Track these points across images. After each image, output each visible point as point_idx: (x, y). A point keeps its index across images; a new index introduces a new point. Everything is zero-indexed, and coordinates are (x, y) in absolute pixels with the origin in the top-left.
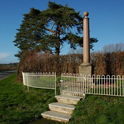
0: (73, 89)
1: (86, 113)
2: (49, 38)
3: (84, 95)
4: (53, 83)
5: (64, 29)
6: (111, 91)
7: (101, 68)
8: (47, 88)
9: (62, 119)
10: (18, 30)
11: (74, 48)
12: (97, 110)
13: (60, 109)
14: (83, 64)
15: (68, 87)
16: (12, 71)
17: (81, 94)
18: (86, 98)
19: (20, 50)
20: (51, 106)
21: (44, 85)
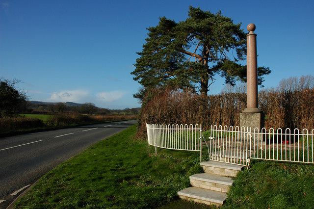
0: (230, 152)
1: (251, 191)
2: (191, 67)
3: (248, 161)
4: (197, 141)
5: (215, 52)
6: (292, 155)
7: (276, 116)
8: (186, 149)
9: (212, 200)
10: (139, 54)
11: (231, 83)
12: (270, 186)
13: (209, 184)
14: (246, 110)
15: (222, 148)
16: (130, 122)
17: (243, 159)
18: (251, 166)
19: (142, 87)
20: (193, 179)
21: (182, 144)
